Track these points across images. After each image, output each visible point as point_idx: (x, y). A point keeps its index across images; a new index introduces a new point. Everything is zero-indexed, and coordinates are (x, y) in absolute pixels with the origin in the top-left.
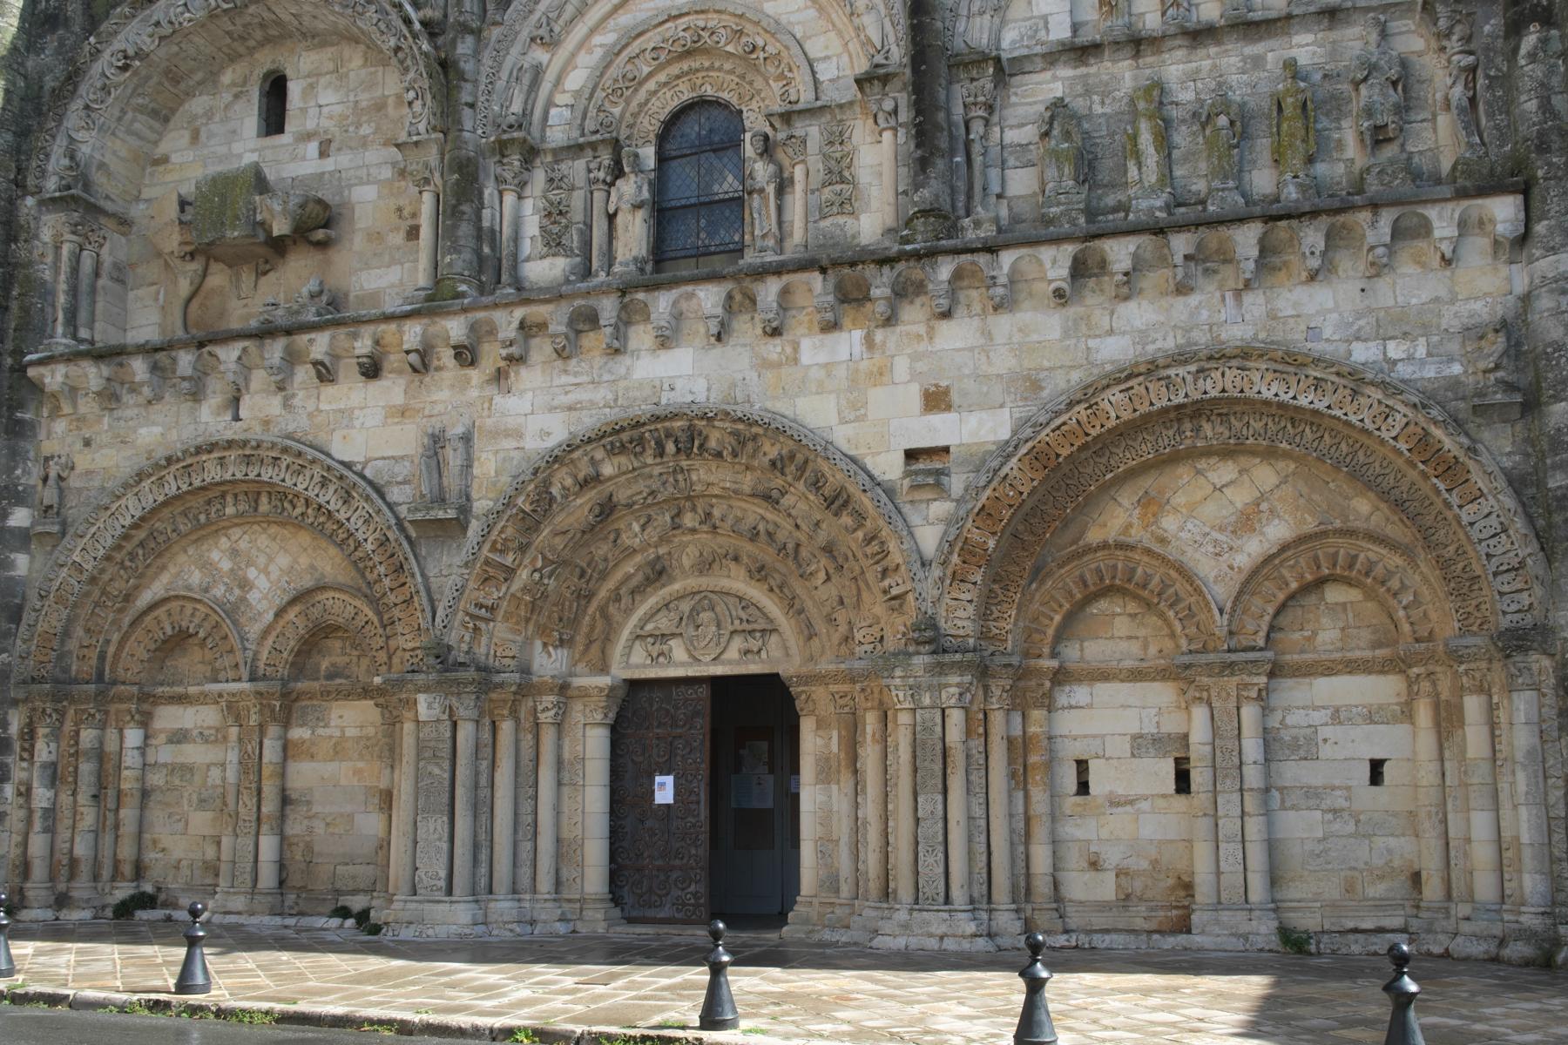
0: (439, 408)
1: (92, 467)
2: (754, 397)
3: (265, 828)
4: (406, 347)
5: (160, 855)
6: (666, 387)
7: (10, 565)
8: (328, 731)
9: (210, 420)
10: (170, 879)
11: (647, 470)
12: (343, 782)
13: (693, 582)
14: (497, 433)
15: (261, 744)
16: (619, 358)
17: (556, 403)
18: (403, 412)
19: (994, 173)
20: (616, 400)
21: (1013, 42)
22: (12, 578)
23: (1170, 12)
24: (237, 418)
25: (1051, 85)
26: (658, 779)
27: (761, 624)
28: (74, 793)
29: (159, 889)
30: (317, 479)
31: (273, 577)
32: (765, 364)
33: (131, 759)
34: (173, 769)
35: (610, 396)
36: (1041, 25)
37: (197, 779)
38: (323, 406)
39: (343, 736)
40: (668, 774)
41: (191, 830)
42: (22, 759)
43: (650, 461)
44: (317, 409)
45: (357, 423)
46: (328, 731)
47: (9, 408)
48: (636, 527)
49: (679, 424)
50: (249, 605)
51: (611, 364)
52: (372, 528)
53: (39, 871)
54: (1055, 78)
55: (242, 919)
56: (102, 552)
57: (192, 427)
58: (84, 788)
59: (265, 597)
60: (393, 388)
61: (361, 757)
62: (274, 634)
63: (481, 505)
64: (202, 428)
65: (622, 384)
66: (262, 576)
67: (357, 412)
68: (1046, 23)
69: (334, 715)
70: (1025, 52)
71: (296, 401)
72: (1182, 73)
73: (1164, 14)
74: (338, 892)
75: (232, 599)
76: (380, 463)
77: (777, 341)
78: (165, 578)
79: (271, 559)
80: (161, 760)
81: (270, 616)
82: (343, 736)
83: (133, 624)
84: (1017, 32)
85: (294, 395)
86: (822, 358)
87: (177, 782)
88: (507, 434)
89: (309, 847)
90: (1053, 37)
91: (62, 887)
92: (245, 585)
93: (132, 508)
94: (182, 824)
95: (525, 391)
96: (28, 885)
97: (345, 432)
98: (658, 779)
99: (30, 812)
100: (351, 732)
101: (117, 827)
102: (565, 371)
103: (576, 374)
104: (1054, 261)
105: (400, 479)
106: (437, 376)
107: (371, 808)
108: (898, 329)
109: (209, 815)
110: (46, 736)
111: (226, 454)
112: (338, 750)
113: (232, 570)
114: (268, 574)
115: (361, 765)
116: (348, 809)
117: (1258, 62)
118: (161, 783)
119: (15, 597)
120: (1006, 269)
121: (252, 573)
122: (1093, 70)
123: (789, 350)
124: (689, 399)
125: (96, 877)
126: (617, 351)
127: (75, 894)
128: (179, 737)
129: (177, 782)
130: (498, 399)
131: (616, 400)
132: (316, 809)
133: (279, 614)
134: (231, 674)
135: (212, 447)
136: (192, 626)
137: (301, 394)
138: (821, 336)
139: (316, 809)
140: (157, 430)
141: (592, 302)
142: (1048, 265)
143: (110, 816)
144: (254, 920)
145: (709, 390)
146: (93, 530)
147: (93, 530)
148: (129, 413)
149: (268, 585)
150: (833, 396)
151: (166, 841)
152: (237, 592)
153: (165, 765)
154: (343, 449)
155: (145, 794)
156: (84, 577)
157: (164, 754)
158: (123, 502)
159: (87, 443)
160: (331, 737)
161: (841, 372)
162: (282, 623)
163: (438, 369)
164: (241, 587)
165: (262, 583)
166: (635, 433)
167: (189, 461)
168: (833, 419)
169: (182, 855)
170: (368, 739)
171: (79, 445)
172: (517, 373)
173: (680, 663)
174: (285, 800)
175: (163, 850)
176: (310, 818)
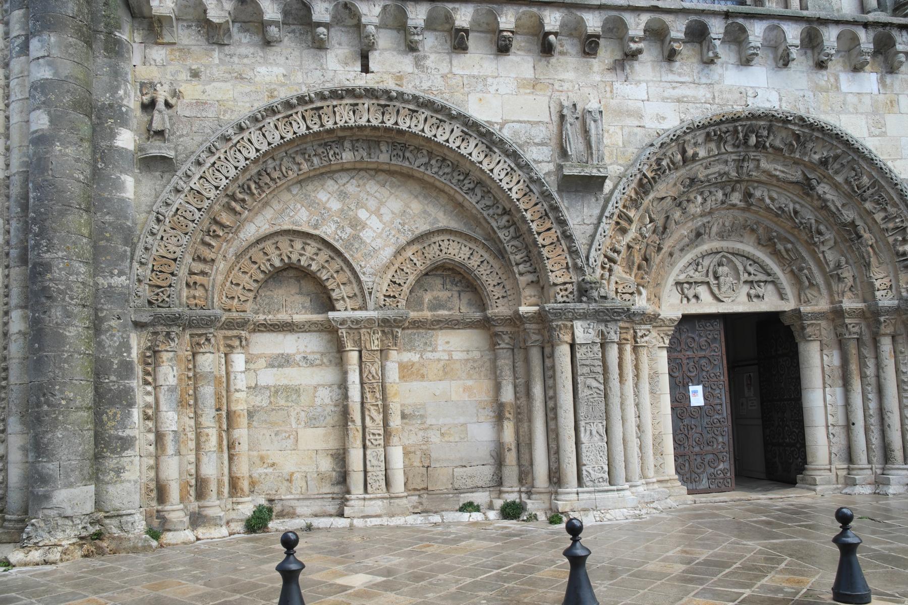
0: (566, 86)
1: (204, 97)
2: (811, 110)
3: (394, 440)
4: (547, 28)
5: (270, 470)
6: (750, 93)
7: (119, 186)
8: (436, 355)
9: (337, 68)
10: (283, 490)
11: (725, 157)
12: (454, 397)
13: (716, 244)
14: (621, 113)
15: (383, 368)
16: (713, 67)
17: (666, 94)
18: (535, 84)
20: (714, 98)
22: (123, 200)
24: (366, 69)
26: (692, 388)
27: (762, 277)
28: (197, 416)
29: (271, 501)
30: (457, 132)
31: (387, 218)
32: (818, 89)
33: (241, 382)
34: (277, 391)
35: (709, 95)
37: (304, 399)
38: (455, 70)
39: (450, 359)
40: (698, 384)
41: (302, 445)
42: (147, 383)
43: (730, 149)
44: (451, 72)
45: (492, 89)
46: (436, 355)
47: (107, 25)
48: (699, 199)
49: (762, 123)
50: (363, 242)
51: (706, 71)
52: (515, 180)
53: (174, 493)
55: (384, 521)
56: (224, 182)
57: (318, 73)
58: (207, 410)
59: (379, 236)
60: (521, 63)
61: (470, 377)
62: (393, 269)
63: (613, 169)
64: (329, 75)
65: (717, 87)
66: (373, 216)
67: (490, 80)
69: (439, 342)
71: (428, 63)
74: (458, 491)
75: (344, 236)
76: (517, 126)
77: (824, 72)
78: (269, 213)
79: (382, 203)
80: (262, 382)
81: (387, 253)
82: (450, 359)
83: (239, 256)
85: (425, 57)
86: (855, 89)
87: (282, 402)
88: (630, 113)
89: (426, 455)
91: (194, 506)
92: (356, 224)
93: (257, 143)
94: (291, 441)
95: (639, 82)
96: (168, 508)
97: (480, 95)
98: (692, 388)
99: (159, 438)
100: (457, 356)
101: (231, 446)
102: (671, 71)
103: (680, 74)
105: (536, 141)
106: (562, 59)
107: (482, 419)
108: (900, 76)
109: (321, 431)
110: (171, 360)
111: (360, 101)
112: (447, 372)
113: (342, 210)
114: (380, 216)
115: (470, 383)
116: (462, 420)
118: (265, 403)
119: (127, 219)
121: (363, 214)
123: (832, 80)
124: (768, 105)
125: (219, 493)
126: (712, 62)
127: (210, 512)
128: (282, 361)
129: (282, 402)
130: (617, 85)
131: (714, 98)
132: (429, 421)
133: (399, 252)
134: (349, 303)
135: (335, 94)
136: (303, 259)
137: (433, 57)
138: (852, 74)
139: (429, 421)
140: (279, 71)
141: (704, 19)
143: (224, 434)
144: (398, 521)
145: (780, 100)
146: (213, 159)
147: (213, 159)
148: (243, 50)
149: (381, 226)
150: (863, 117)
151: (274, 456)
152: (349, 230)
153: (267, 388)
154: (478, 112)
155: (251, 414)
156: (206, 203)
157: (268, 377)
158: (246, 135)
159: (195, 74)
160: (439, 360)
161: (867, 100)
162: (400, 259)
163: (562, 53)
164: (353, 226)
165: (374, 223)
166: (730, 127)
167: (319, 104)
168: (866, 135)
169: (293, 469)
170: (475, 361)
171: (184, 75)
172: (632, 67)
173: (707, 305)
174: (404, 416)
175: (273, 465)
176: (425, 429)
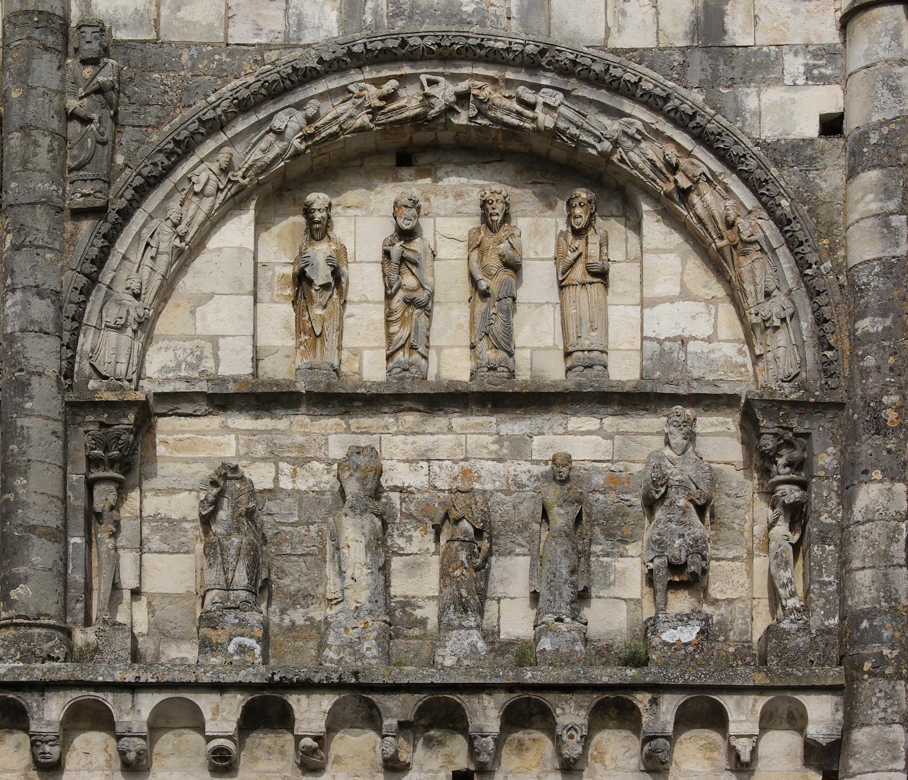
19: (127, 560)
21: (164, 369)
23: (400, 356)
25: (221, 438)
36: (208, 348)
54: (226, 429)
68: (216, 348)
70: (182, 387)
72: (417, 455)
73: (389, 357)
84: (170, 354)
90: (225, 371)
104: (216, 711)
117: (518, 448)
120: (145, 714)
122: (282, 424)
142: (207, 716)
